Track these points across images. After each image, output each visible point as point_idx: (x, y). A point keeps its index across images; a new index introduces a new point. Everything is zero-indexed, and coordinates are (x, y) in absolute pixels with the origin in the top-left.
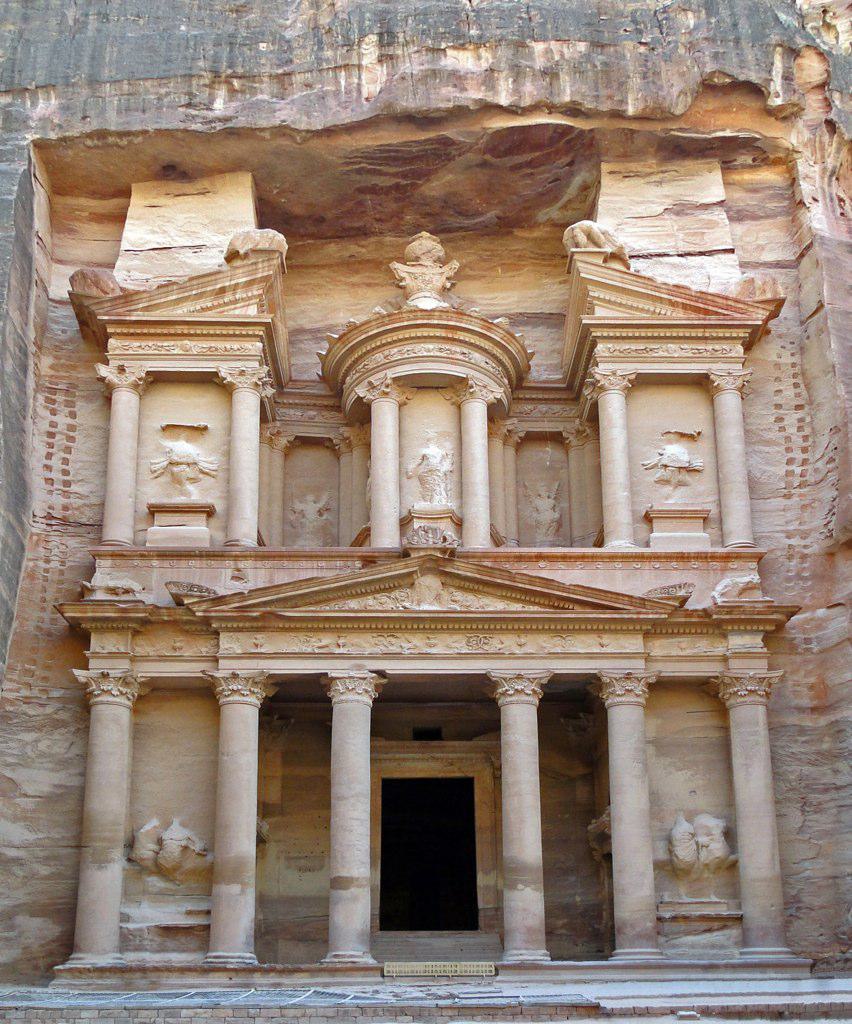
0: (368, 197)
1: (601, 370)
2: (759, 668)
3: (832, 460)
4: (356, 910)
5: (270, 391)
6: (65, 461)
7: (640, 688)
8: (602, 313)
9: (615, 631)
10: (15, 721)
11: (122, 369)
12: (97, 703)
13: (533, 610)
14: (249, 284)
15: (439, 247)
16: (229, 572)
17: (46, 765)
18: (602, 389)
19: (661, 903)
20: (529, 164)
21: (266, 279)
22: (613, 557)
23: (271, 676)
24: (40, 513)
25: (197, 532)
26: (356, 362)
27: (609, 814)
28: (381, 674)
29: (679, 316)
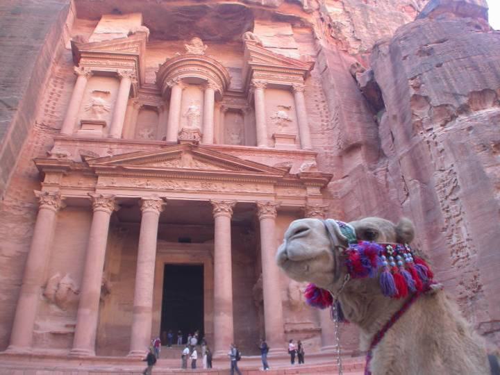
0: (179, 25)
1: (255, 81)
2: (318, 203)
3: (337, 119)
4: (145, 326)
5: (135, 82)
6: (54, 104)
7: (273, 210)
8: (254, 62)
9: (263, 183)
10: (7, 216)
11: (83, 69)
12: (43, 208)
13: (228, 172)
14: (134, 43)
15: (201, 42)
16: (107, 150)
17: (16, 241)
18: (256, 87)
19: (286, 324)
20: (231, 18)
21: (139, 42)
22: (261, 151)
23: (117, 199)
24: (39, 122)
25: (98, 132)
26: (168, 73)
27: (262, 278)
28: (164, 199)
29: (281, 65)
